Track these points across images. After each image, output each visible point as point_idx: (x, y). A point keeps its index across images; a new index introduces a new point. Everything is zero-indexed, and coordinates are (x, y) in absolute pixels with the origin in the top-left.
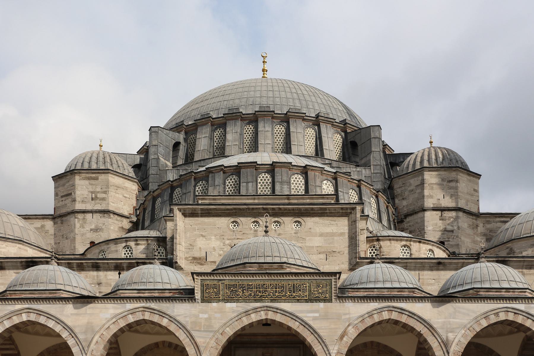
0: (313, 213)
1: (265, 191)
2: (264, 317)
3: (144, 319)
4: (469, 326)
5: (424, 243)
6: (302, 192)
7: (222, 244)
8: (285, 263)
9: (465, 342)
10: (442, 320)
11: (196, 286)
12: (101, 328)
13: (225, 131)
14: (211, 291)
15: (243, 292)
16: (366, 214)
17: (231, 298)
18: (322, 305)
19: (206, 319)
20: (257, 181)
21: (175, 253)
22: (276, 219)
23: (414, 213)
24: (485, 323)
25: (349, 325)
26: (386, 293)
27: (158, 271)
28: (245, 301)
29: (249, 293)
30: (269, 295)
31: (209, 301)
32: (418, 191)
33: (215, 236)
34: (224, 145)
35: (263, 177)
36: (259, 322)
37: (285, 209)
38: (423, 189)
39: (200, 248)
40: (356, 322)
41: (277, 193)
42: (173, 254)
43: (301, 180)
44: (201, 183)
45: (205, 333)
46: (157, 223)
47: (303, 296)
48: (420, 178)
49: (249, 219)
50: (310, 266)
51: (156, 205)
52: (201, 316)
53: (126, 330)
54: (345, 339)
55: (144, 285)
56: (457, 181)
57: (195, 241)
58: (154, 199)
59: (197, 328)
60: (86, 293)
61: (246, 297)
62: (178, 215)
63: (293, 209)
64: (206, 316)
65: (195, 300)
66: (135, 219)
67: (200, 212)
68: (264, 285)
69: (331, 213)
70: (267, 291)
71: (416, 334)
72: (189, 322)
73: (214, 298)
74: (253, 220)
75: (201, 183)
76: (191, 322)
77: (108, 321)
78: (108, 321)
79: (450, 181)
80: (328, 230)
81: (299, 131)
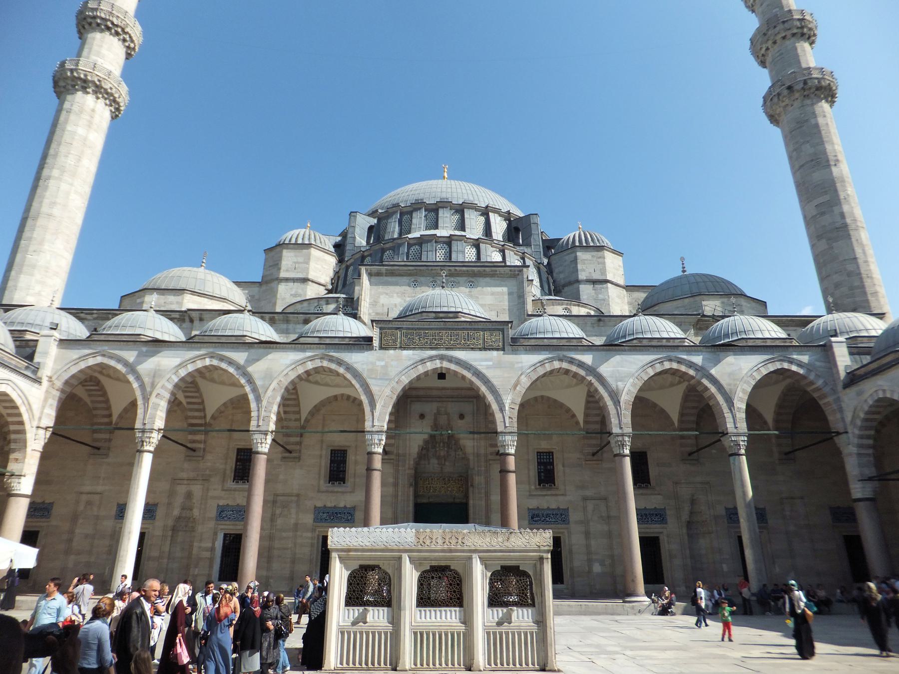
0: (485, 274)
2: (439, 365)
3: (322, 366)
4: (636, 374)
5: (582, 307)
7: (403, 301)
8: (460, 312)
9: (635, 391)
10: (612, 369)
11: (375, 336)
12: (279, 375)
13: (412, 217)
16: (530, 278)
18: (495, 353)
19: (382, 367)
21: (359, 309)
22: (452, 279)
23: (570, 283)
24: (651, 372)
25: (521, 374)
26: (555, 342)
27: (341, 320)
28: (421, 349)
29: (425, 341)
31: (386, 349)
33: (397, 293)
34: (410, 228)
36: (435, 370)
37: (460, 271)
38: (576, 264)
39: (383, 305)
40: (529, 371)
41: (453, 260)
42: (357, 310)
45: (380, 381)
46: (347, 288)
48: (573, 255)
49: (428, 278)
50: (483, 316)
52: (378, 363)
53: (304, 378)
54: (518, 388)
55: (326, 333)
56: (604, 258)
57: (379, 297)
58: (347, 268)
59: (373, 376)
60: (268, 339)
62: (365, 278)
63: (468, 271)
64: (383, 363)
65: (373, 347)
66: (330, 287)
67: (384, 272)
69: (502, 274)
71: (587, 383)
72: (366, 370)
74: (432, 280)
76: (368, 370)
77: (288, 367)
78: (288, 367)
81: (472, 217)
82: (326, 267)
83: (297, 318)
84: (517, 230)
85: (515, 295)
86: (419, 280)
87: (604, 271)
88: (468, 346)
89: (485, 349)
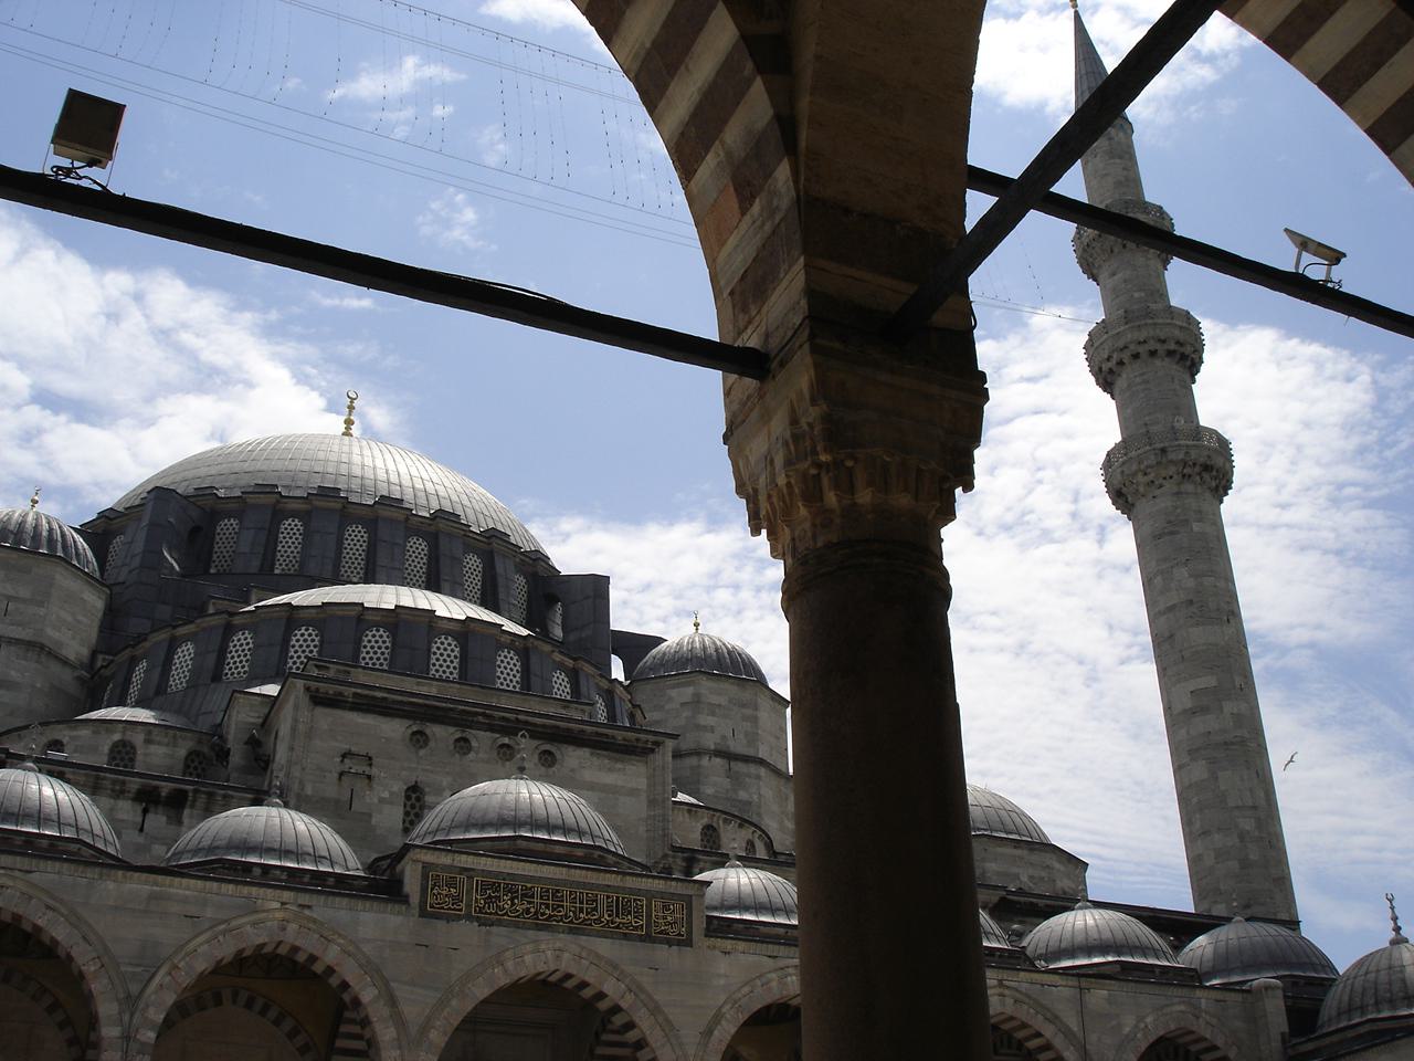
1: (444, 672)
6: (514, 687)
14: (444, 892)
15: (513, 904)
17: (486, 913)
20: (429, 650)
28: (517, 926)
30: (566, 916)
32: (686, 713)
35: (442, 643)
43: (515, 661)
44: (303, 631)
47: (636, 928)
48: (690, 690)
49: (452, 729)
51: (176, 657)
54: (716, 1032)
61: (518, 917)
63: (544, 726)
68: (558, 891)
70: (562, 906)
73: (450, 909)
75: (303, 631)
79: (744, 706)
80: (609, 779)
82: (85, 620)
83: (124, 783)
84: (551, 600)
85: (643, 797)
86: (428, 731)
87: (753, 739)
88: (617, 927)
89: (648, 938)
